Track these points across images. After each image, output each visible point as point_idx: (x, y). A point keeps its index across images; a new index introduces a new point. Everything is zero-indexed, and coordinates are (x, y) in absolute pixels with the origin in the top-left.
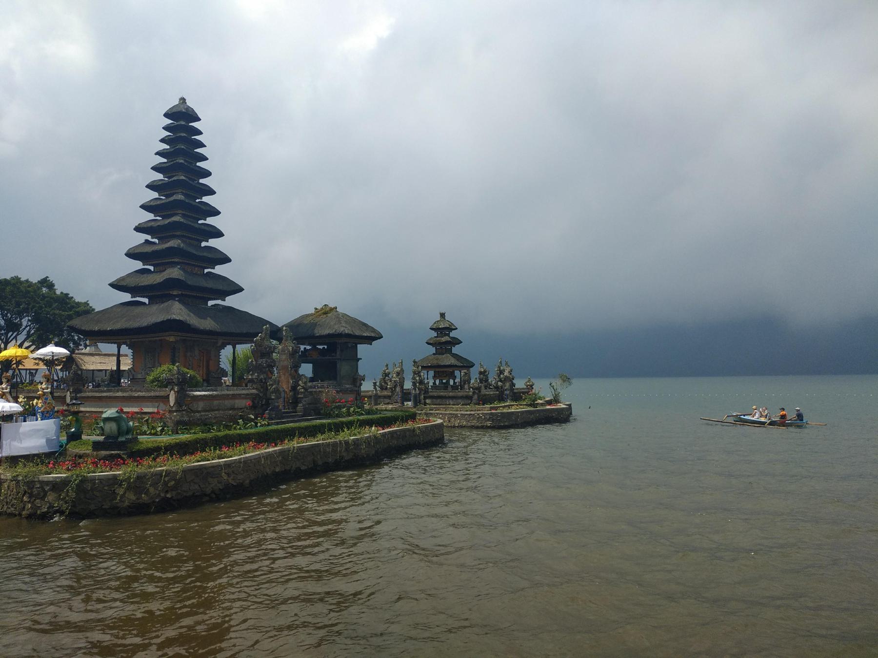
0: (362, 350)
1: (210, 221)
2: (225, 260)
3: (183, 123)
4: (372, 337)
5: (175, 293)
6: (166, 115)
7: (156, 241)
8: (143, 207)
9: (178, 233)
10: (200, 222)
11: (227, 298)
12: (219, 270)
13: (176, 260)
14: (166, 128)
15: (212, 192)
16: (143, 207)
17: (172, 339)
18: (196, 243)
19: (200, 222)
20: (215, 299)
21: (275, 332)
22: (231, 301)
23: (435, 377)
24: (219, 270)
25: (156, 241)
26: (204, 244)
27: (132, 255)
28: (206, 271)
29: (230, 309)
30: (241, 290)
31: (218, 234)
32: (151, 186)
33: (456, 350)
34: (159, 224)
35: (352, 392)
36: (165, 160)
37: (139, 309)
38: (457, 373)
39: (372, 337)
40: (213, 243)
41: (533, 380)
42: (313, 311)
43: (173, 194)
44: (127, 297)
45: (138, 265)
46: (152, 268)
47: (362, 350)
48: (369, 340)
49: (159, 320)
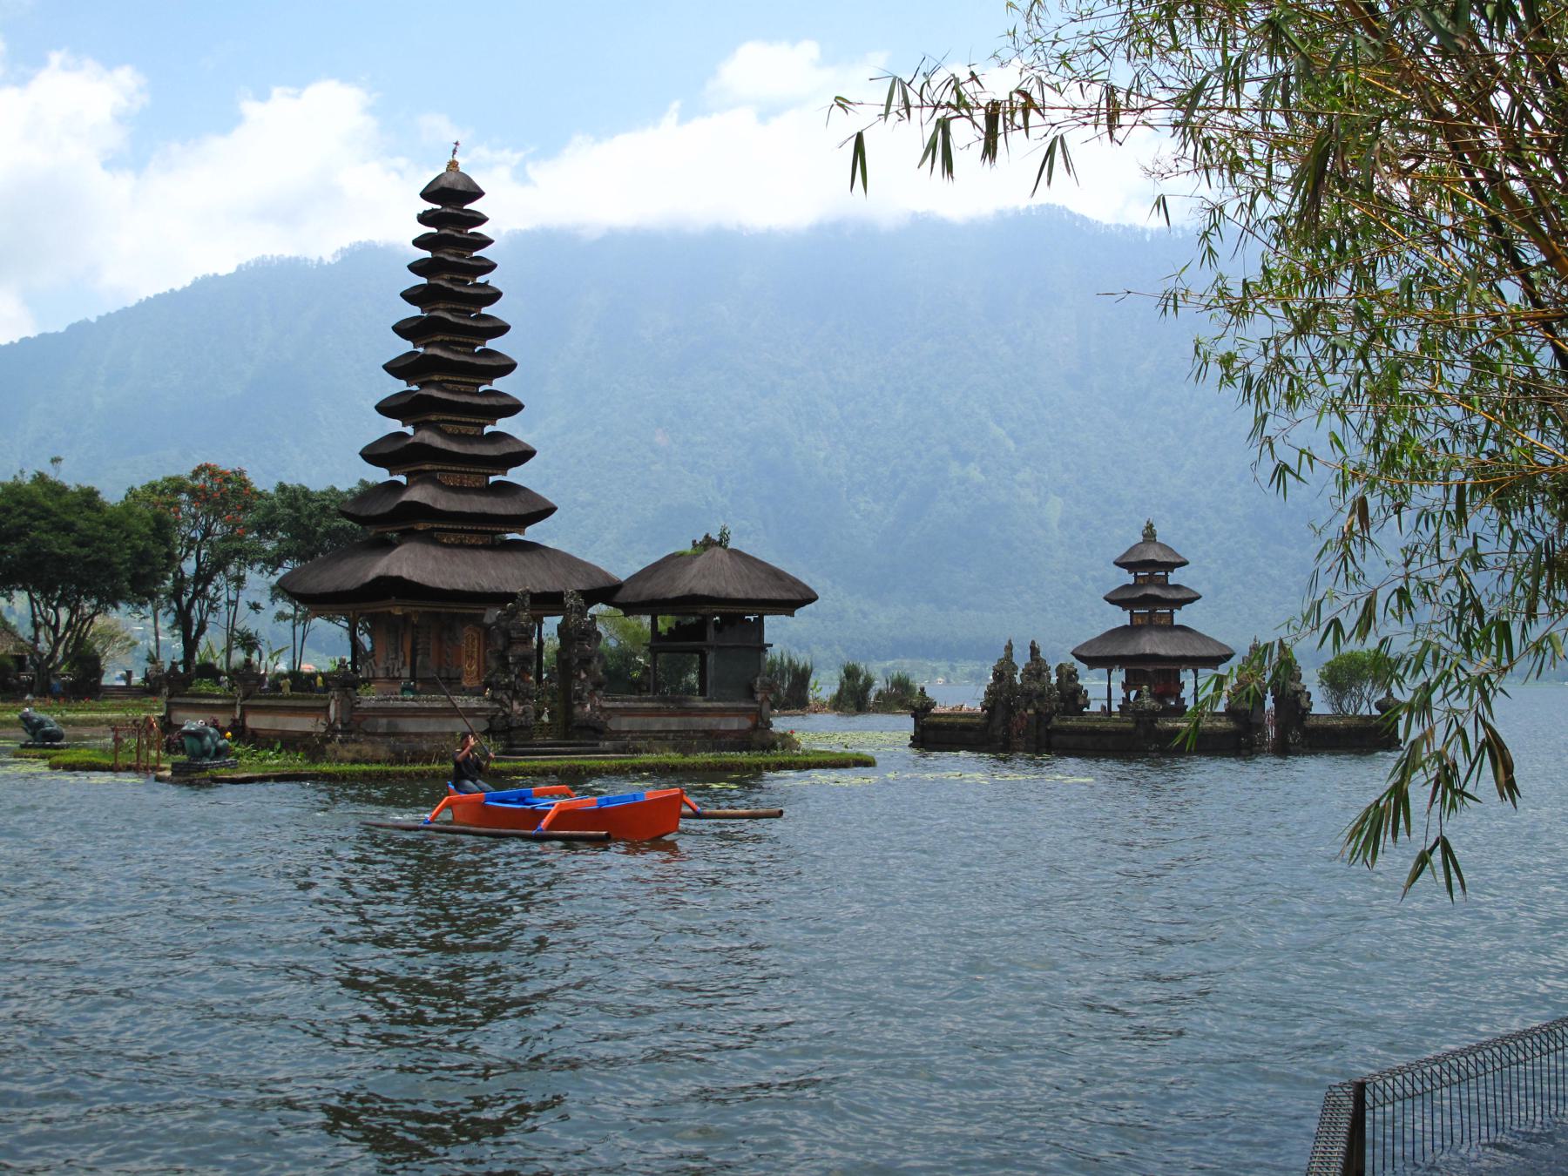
0: (775, 628)
1: (499, 384)
4: (795, 599)
5: (421, 527)
6: (426, 195)
7: (409, 430)
10: (481, 389)
11: (529, 529)
12: (514, 475)
14: (424, 219)
15: (502, 329)
17: (398, 612)
18: (472, 431)
19: (481, 389)
21: (607, 592)
23: (1126, 687)
25: (409, 430)
28: (492, 479)
30: (549, 510)
31: (513, 408)
32: (402, 329)
33: (1180, 617)
35: (738, 712)
36: (424, 281)
38: (1187, 677)
39: (795, 599)
46: (403, 479)
47: (775, 628)
48: (788, 606)
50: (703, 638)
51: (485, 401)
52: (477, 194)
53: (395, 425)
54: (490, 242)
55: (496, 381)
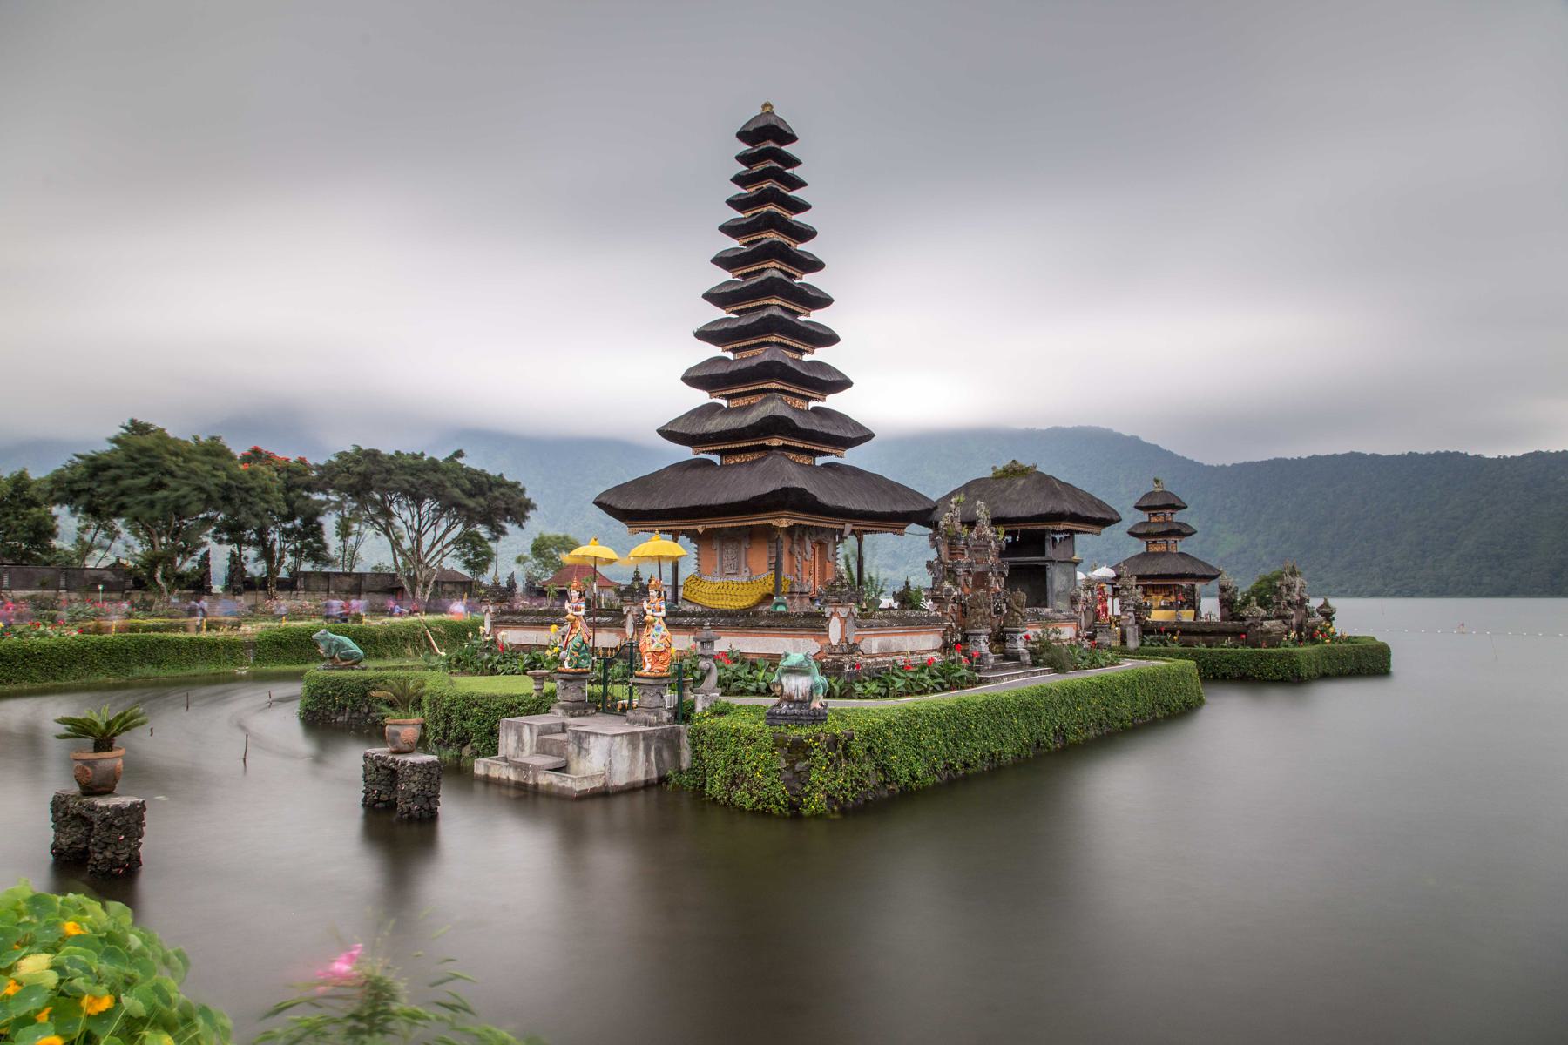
0: (1085, 543)
2: (843, 384)
3: (772, 144)
6: (743, 136)
7: (730, 355)
8: (710, 297)
9: (774, 339)
12: (833, 402)
13: (774, 386)
16: (710, 297)
20: (828, 454)
22: (851, 457)
24: (833, 402)
25: (730, 355)
26: (806, 358)
27: (694, 379)
28: (812, 404)
29: (856, 472)
34: (735, 326)
37: (710, 472)
40: (821, 354)
41: (1333, 602)
42: (990, 474)
43: (763, 270)
44: (686, 453)
45: (702, 398)
46: (724, 403)
49: (1340, 451)
50: (1043, 554)
51: (804, 329)
52: (792, 138)
53: (715, 351)
54: (803, 184)
55: (813, 313)
